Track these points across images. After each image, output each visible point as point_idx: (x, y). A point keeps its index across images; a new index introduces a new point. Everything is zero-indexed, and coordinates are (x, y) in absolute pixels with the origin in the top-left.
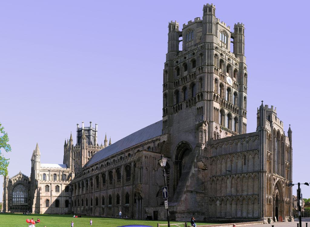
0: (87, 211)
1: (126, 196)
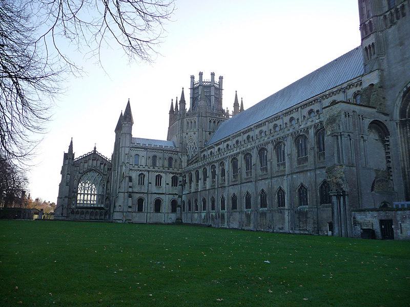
0: (213, 219)
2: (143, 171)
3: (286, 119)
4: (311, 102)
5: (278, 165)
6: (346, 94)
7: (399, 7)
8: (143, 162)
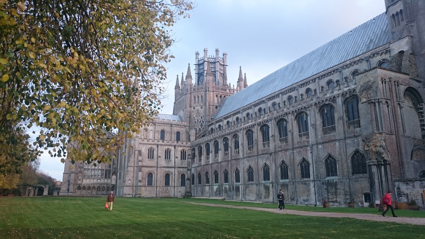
0: (226, 192)
1: (326, 161)
2: (153, 144)
3: (302, 90)
4: (330, 73)
5: (300, 136)
6: (370, 63)
8: (151, 136)
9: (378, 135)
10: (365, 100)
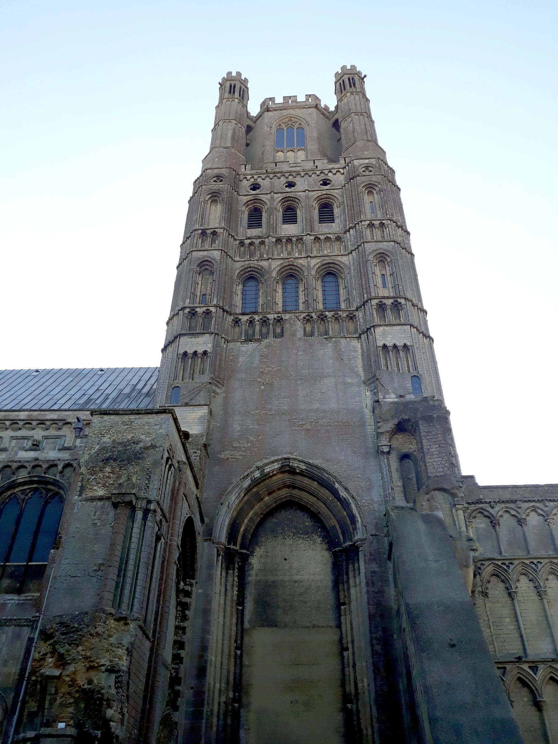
7: (271, 317)
9: (112, 623)
10: (101, 492)
